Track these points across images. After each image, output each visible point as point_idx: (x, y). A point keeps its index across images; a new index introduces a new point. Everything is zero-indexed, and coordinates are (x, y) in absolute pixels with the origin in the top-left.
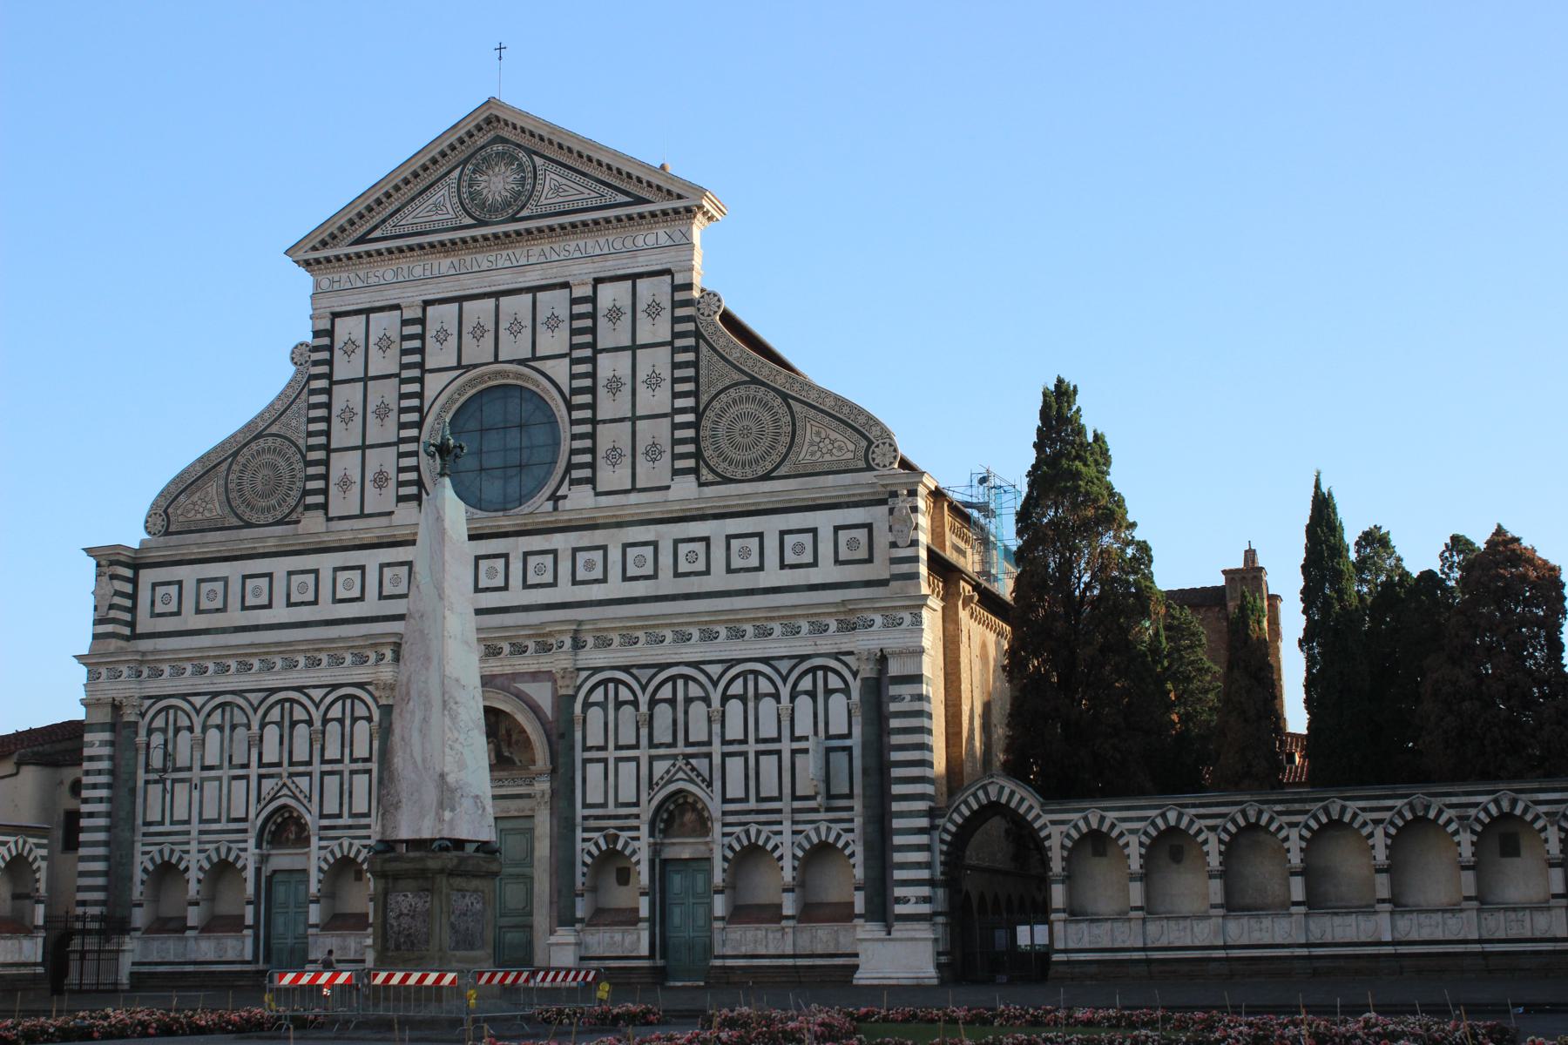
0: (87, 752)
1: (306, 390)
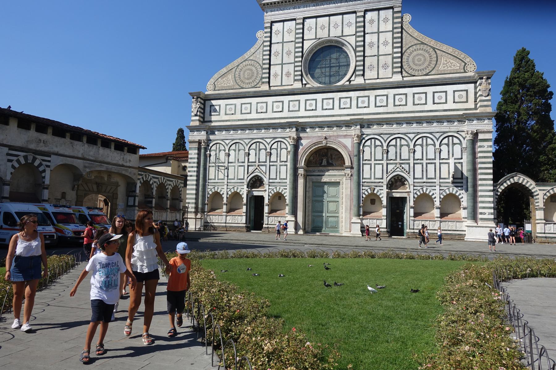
0: (190, 156)
1: (262, 46)
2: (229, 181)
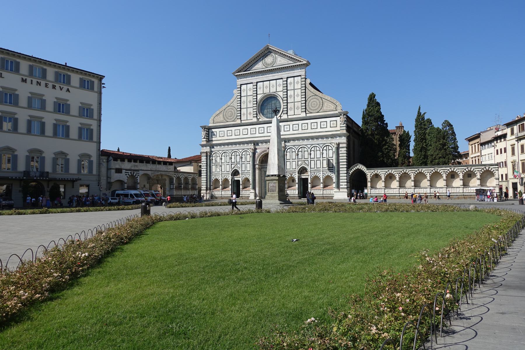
0: (202, 160)
2: (222, 173)
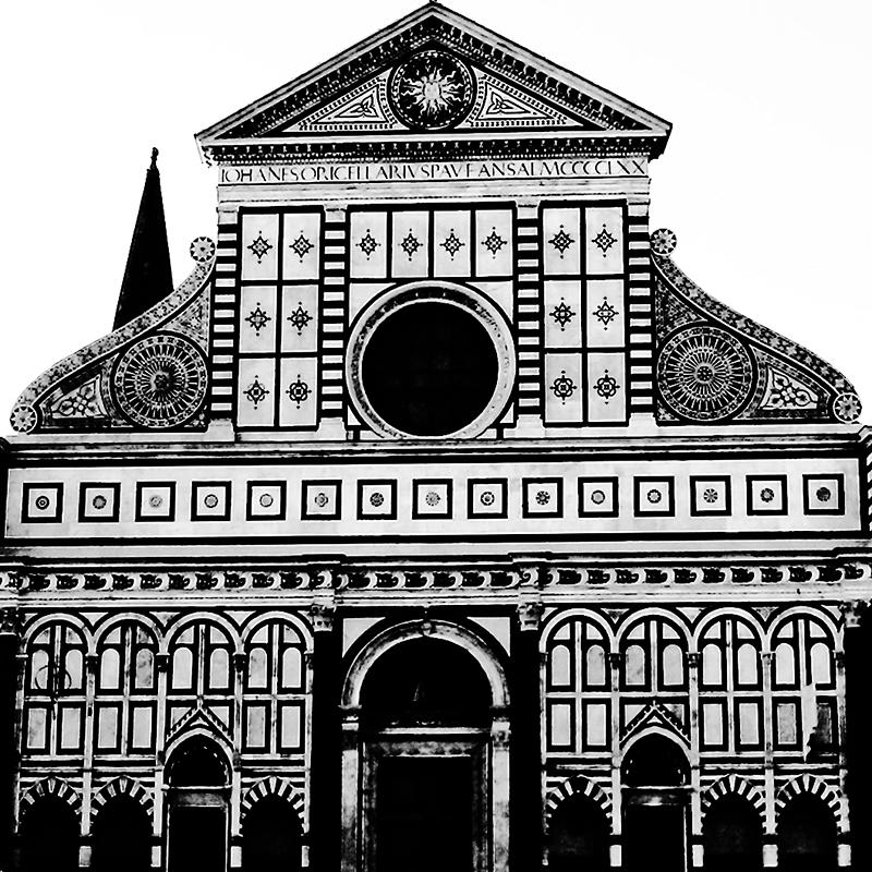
1: (209, 288)
